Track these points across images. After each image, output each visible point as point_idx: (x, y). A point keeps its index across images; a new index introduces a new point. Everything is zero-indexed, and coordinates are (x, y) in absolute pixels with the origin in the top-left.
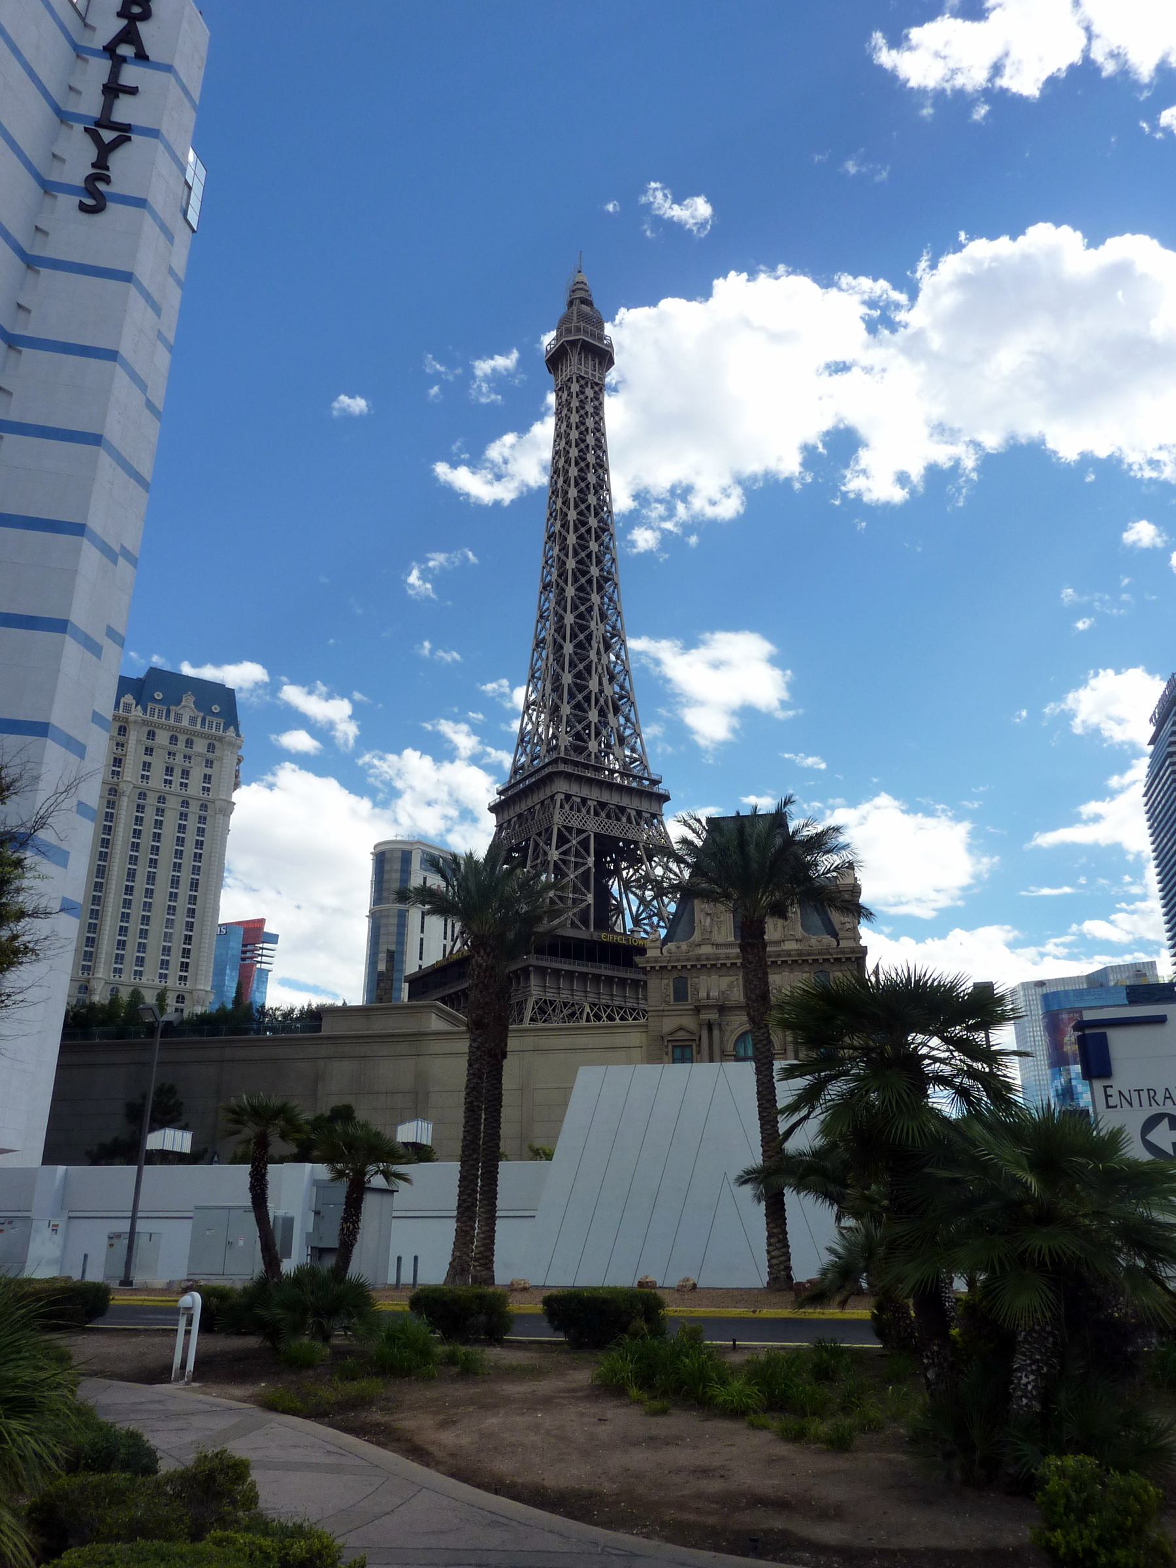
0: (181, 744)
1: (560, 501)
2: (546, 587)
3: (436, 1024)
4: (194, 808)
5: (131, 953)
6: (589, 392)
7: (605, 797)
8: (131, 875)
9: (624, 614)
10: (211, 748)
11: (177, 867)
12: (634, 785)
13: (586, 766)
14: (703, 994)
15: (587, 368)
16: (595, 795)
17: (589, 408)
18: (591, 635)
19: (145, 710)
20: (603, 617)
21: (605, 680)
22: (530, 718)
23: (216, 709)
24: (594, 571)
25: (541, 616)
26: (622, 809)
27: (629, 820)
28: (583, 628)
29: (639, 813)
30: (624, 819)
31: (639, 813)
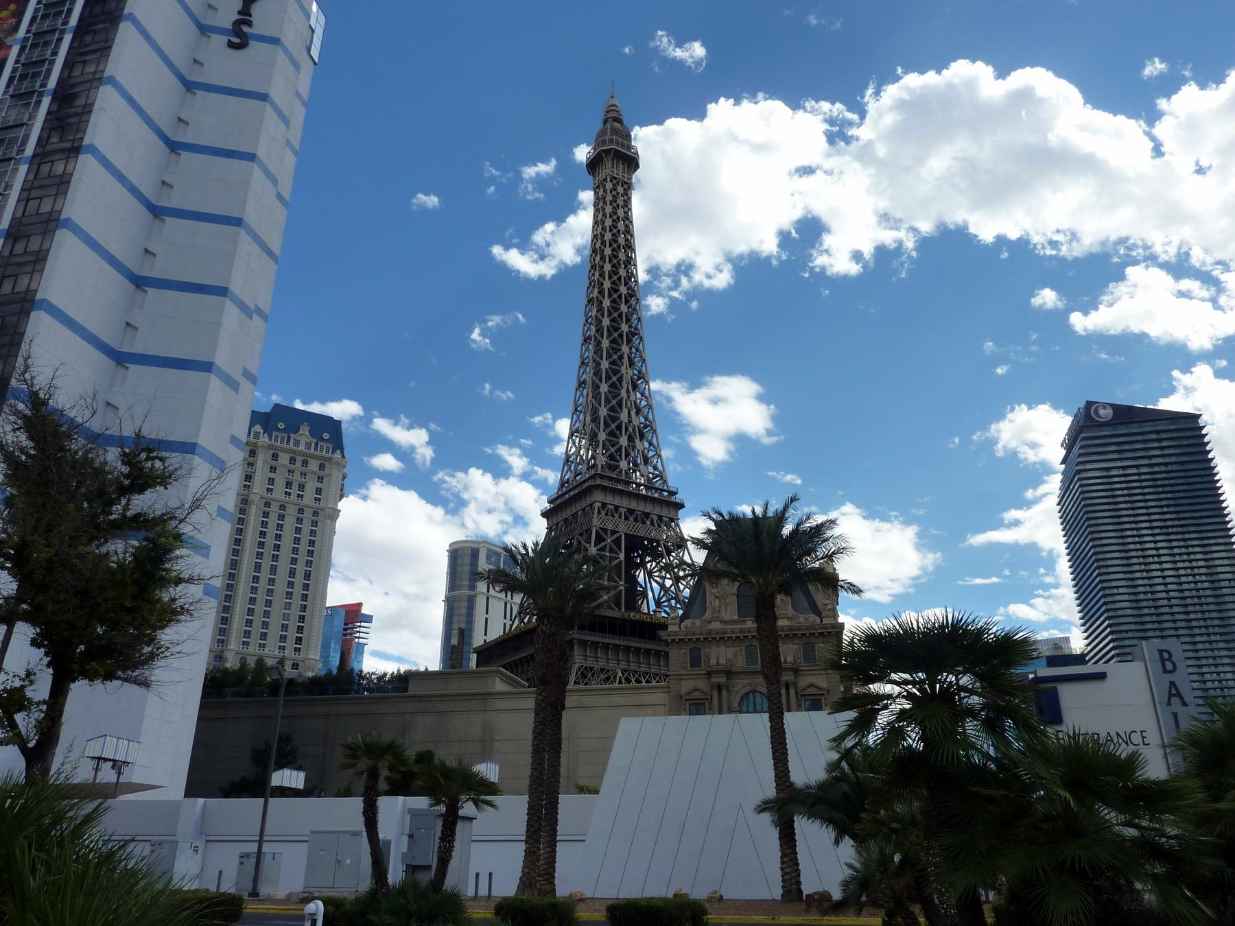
0: (298, 464)
1: (597, 274)
2: (586, 340)
3: (499, 686)
4: (308, 515)
5: (256, 629)
6: (620, 189)
7: (633, 505)
8: (258, 567)
9: (648, 361)
10: (322, 467)
11: (294, 561)
12: (656, 495)
13: (618, 481)
14: (713, 662)
15: (619, 172)
16: (625, 503)
17: (620, 201)
18: (621, 377)
19: (270, 438)
20: (631, 363)
21: (633, 413)
22: (574, 443)
23: (326, 436)
24: (624, 328)
25: (583, 363)
26: (647, 515)
27: (652, 523)
28: (616, 372)
29: (660, 518)
30: (648, 523)
31: (660, 518)
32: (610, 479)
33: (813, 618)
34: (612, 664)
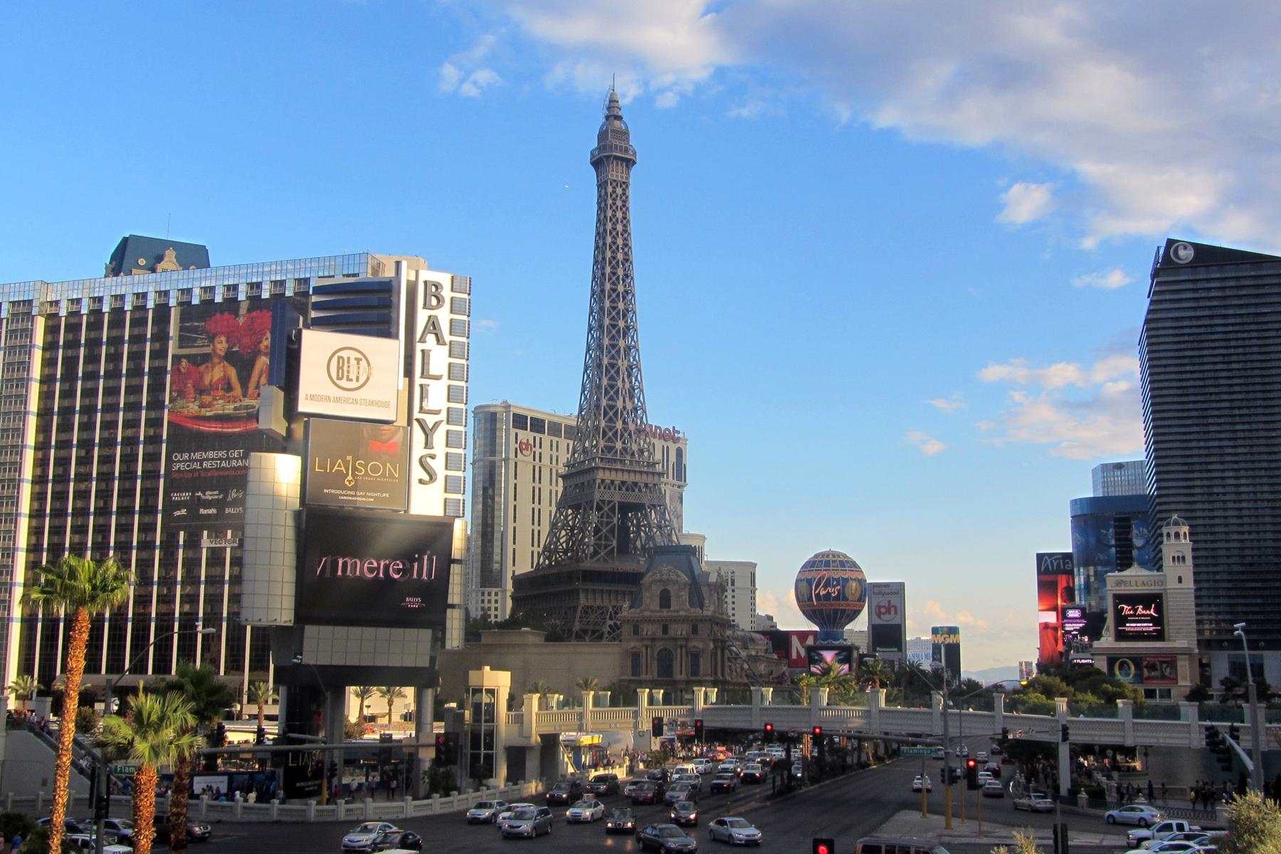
6: (619, 191)
7: (626, 477)
13: (615, 461)
17: (619, 203)
26: (635, 484)
28: (613, 366)
32: (609, 460)
33: (699, 610)
34: (606, 603)
